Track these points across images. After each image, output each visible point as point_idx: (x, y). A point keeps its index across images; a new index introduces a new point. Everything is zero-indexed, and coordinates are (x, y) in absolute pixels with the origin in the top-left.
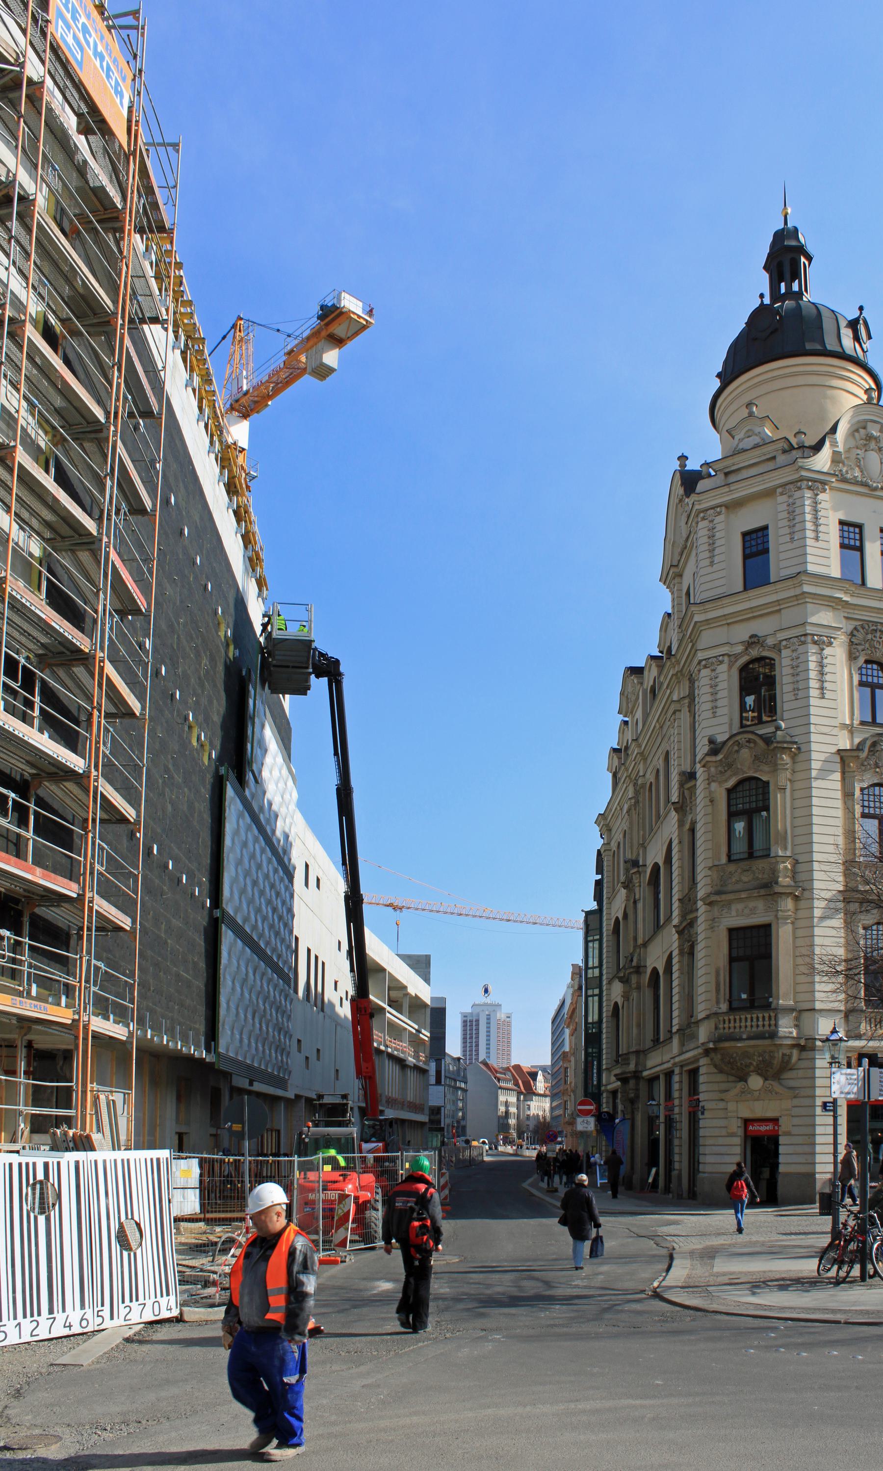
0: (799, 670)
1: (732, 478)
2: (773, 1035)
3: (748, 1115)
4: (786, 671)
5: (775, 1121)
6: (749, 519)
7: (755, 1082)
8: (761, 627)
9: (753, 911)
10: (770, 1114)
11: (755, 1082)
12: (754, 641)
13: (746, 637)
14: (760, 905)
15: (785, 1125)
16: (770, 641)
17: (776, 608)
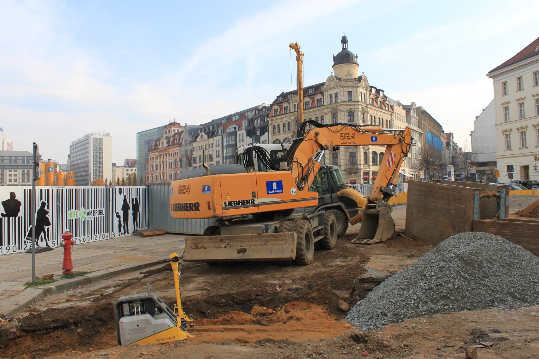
0: (358, 115)
1: (347, 83)
2: (358, 168)
3: (351, 179)
4: (356, 115)
5: (355, 180)
6: (350, 89)
7: (353, 175)
8: (352, 107)
9: (354, 150)
10: (355, 179)
11: (353, 175)
12: (350, 109)
13: (349, 108)
14: (355, 149)
15: (357, 181)
16: (353, 110)
17: (354, 105)
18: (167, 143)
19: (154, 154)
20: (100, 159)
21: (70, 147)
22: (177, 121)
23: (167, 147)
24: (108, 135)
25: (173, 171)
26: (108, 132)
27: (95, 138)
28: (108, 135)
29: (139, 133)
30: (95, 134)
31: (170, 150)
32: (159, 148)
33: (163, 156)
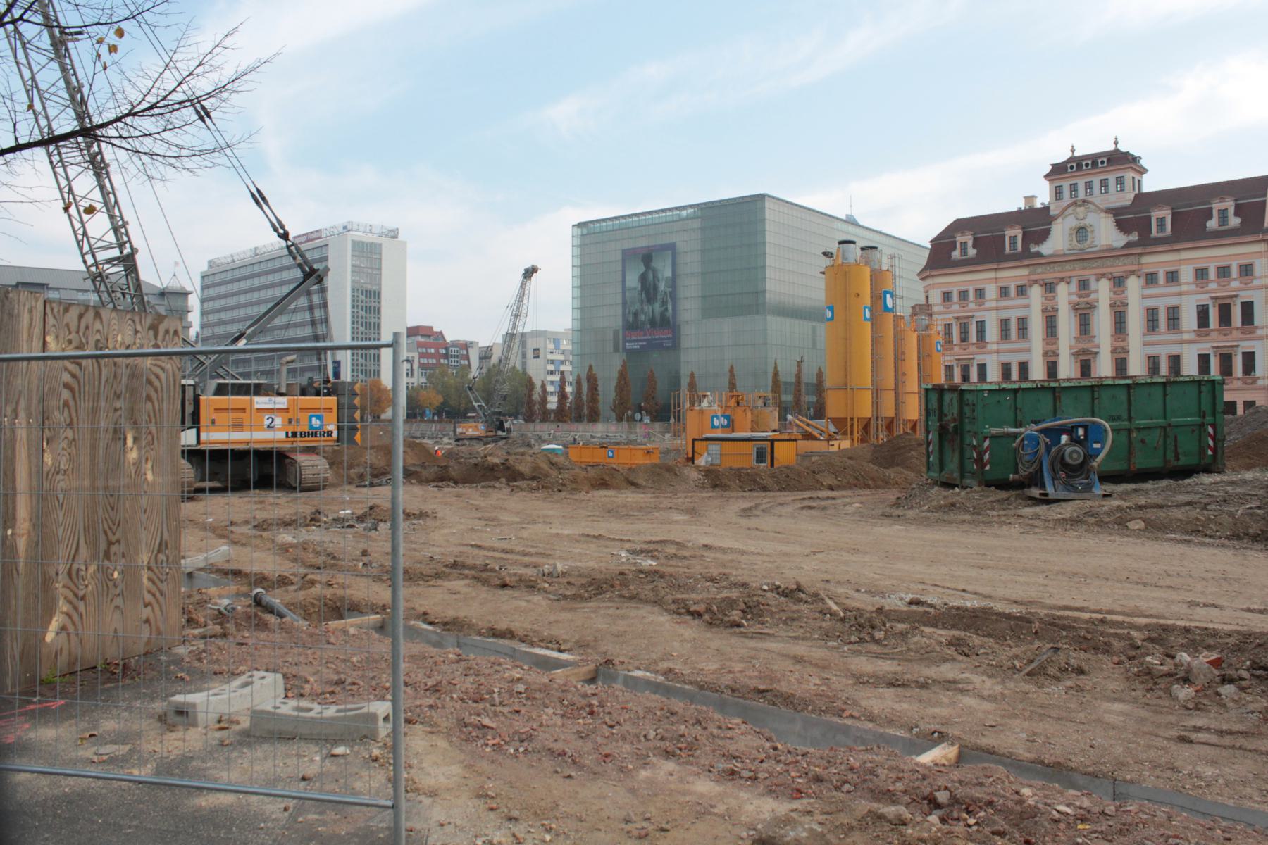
18: (1123, 226)
19: (991, 275)
20: (373, 315)
21: (203, 277)
22: (1123, 148)
23: (1129, 245)
24: (394, 234)
25: (1190, 342)
26: (394, 226)
27: (359, 242)
28: (394, 234)
29: (580, 225)
30: (358, 230)
31: (1145, 260)
32: (1039, 255)
33: (1084, 284)
